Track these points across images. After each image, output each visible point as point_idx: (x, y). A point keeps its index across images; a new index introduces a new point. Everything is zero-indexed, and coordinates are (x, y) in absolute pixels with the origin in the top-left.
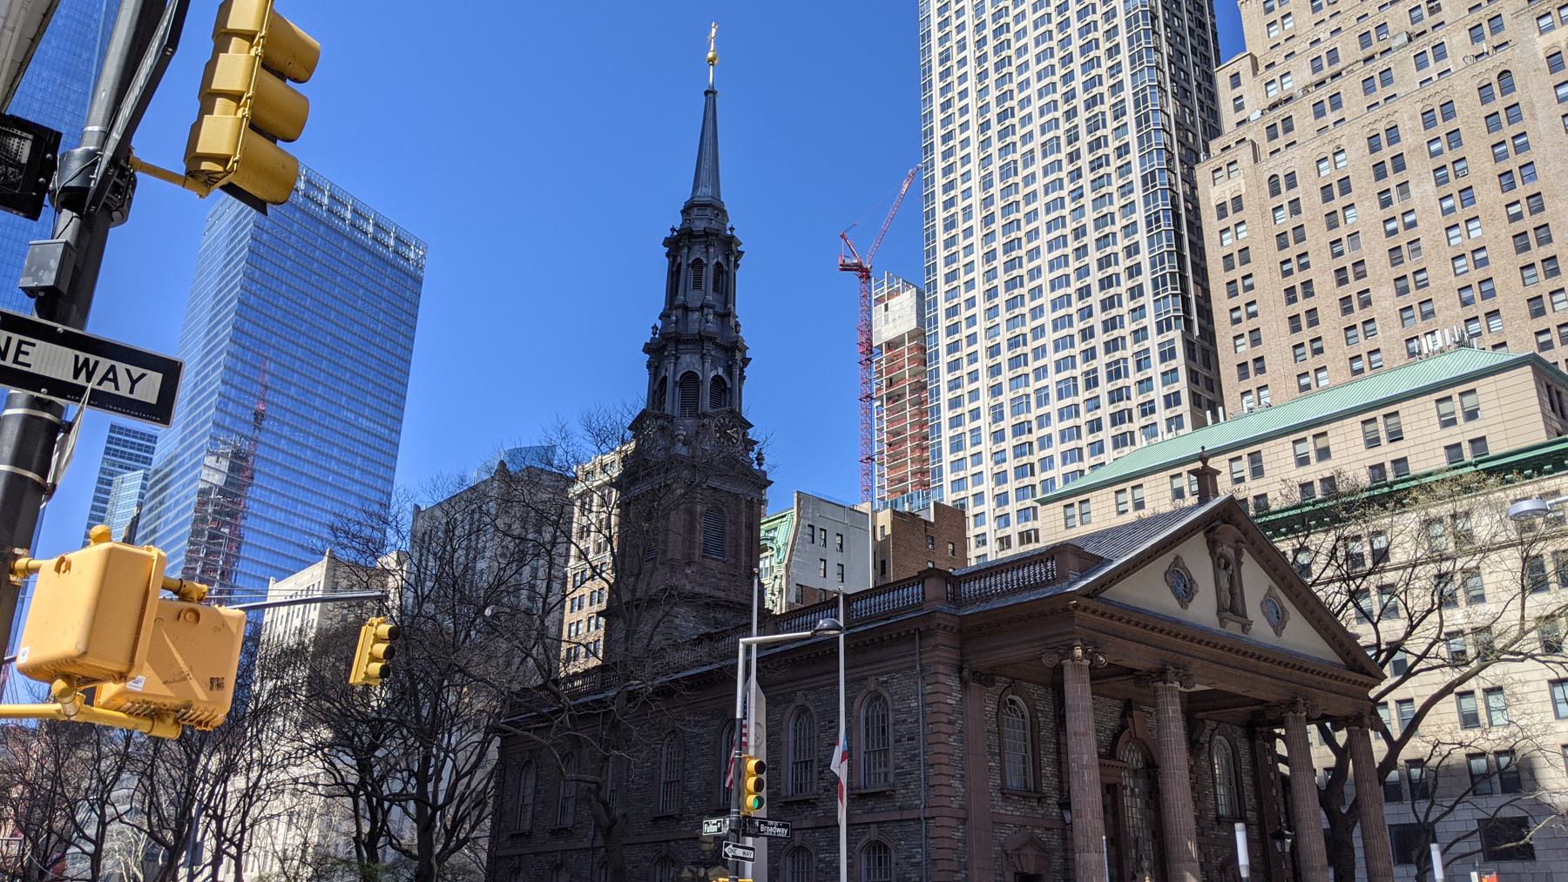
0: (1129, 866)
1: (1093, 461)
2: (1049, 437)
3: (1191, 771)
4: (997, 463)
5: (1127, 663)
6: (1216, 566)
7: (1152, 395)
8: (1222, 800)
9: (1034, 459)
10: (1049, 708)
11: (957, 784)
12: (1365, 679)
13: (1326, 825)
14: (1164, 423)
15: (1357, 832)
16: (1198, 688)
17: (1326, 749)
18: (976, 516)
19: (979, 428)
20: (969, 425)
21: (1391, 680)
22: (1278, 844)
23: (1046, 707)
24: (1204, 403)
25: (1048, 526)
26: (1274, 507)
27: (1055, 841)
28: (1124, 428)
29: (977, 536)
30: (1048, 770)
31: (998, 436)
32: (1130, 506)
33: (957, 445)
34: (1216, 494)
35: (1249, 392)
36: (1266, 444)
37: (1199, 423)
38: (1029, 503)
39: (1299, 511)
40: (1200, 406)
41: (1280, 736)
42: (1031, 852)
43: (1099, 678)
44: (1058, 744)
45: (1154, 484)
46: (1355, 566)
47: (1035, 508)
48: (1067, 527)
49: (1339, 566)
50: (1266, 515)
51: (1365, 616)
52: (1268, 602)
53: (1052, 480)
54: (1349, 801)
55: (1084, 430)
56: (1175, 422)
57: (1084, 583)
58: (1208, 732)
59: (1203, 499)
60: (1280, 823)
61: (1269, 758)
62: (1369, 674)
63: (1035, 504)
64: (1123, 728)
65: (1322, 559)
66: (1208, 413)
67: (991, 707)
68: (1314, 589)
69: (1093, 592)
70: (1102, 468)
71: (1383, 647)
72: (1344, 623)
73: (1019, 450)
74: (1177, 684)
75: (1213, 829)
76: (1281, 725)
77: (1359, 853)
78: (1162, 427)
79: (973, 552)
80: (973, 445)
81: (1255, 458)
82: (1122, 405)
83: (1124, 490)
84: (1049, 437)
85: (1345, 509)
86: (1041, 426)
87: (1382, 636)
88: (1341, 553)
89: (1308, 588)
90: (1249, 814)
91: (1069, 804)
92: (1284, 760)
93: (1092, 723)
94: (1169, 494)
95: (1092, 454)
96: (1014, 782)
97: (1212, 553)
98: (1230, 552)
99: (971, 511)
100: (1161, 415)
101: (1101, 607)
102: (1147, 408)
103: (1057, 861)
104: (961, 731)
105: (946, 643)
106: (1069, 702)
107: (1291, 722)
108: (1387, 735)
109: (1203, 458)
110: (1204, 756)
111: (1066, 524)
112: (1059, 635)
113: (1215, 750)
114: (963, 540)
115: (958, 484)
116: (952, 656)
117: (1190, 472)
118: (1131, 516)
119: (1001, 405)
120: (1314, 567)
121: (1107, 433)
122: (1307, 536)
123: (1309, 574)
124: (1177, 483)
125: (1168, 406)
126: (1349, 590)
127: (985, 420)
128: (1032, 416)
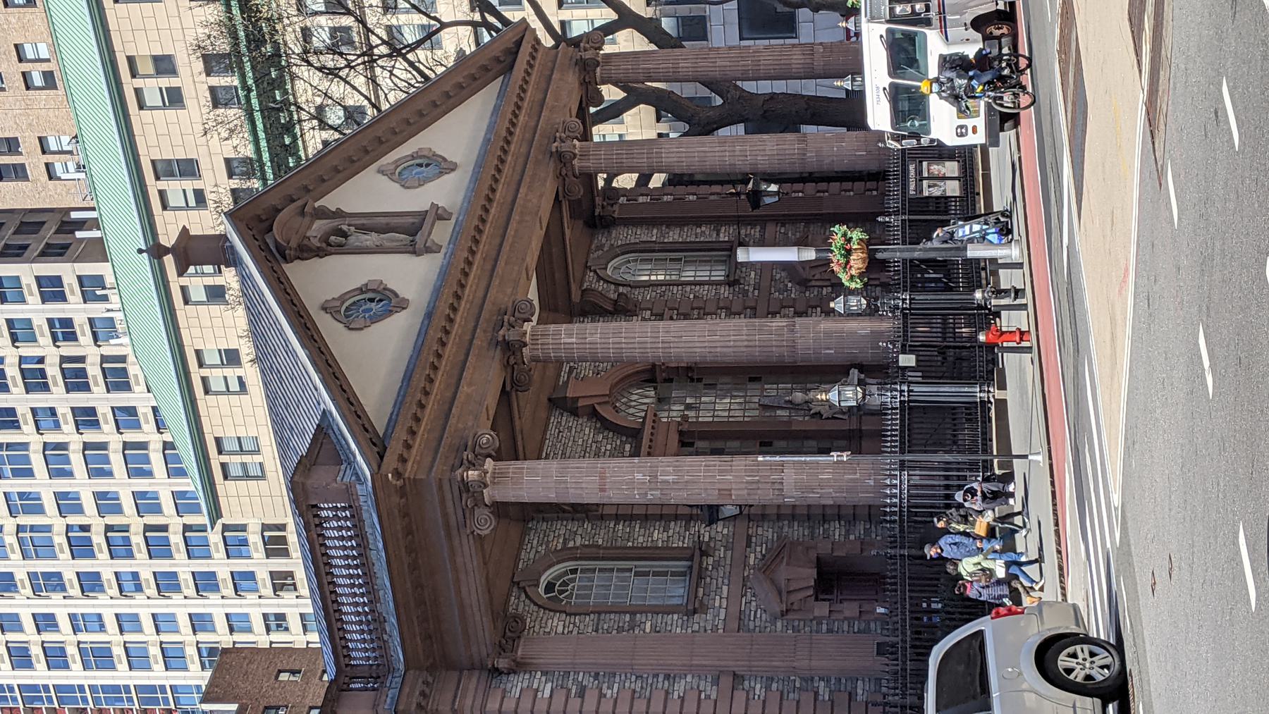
0: (801, 421)
1: (149, 426)
2: (99, 496)
3: (660, 317)
4: (139, 588)
5: (492, 400)
6: (341, 249)
7: (39, 322)
8: (703, 274)
9: (136, 524)
10: (561, 528)
11: (679, 688)
12: (526, 49)
13: (741, 128)
14: (89, 306)
15: (750, 86)
16: (533, 294)
17: (627, 116)
18: (232, 630)
19: (72, 617)
20: (65, 635)
21: (528, 13)
22: (768, 200)
23: (559, 533)
24: (61, 239)
25: (257, 508)
26: (249, 151)
27: (767, 533)
28: (93, 371)
29: (268, 630)
30: (658, 536)
31: (90, 583)
32: (232, 373)
33: (99, 657)
34: (224, 237)
35: (48, 166)
36: (142, 150)
37: (98, 251)
38: (215, 537)
39: (257, 115)
40: (66, 247)
41: (608, 181)
42: (783, 573)
43: (516, 451)
44: (617, 518)
45: (196, 332)
46: (351, 43)
47: (226, 528)
48: (262, 477)
49: (348, 66)
50: (262, 165)
51: (429, 37)
52: (400, 175)
53: (176, 495)
54: (704, 92)
55: (91, 436)
56: (91, 288)
57: (359, 458)
58: (601, 286)
59: (229, 258)
60: (738, 194)
61: (641, 199)
62: (519, 43)
63: (218, 527)
64: (594, 414)
65: (337, 89)
66: (79, 234)
67: (557, 623)
68: (385, 106)
69: (377, 446)
70: (164, 412)
71: (477, 17)
72: (440, 70)
73: (119, 547)
74: (527, 327)
75: (746, 293)
76: (590, 178)
77: (780, 87)
78: (97, 310)
79: (297, 637)
80: (102, 628)
81: (165, 169)
82: (53, 371)
83: (204, 380)
84: (99, 496)
85: (258, 47)
86: (79, 510)
87: (460, 17)
88: (329, 61)
89: (382, 117)
90: (723, 237)
91: (710, 507)
92: (644, 179)
93: (585, 463)
94: (215, 309)
95: (137, 426)
96: (677, 592)
97: (320, 253)
98: (319, 227)
99: (223, 638)
100: (76, 309)
101: (401, 434)
102: (63, 330)
103: (796, 532)
104: (597, 676)
105: (449, 696)
106: (551, 497)
107: (590, 164)
108: (609, 29)
109: (156, 251)
110: (637, 294)
111: (256, 478)
112: (443, 501)
113: (629, 278)
114: (273, 652)
115: (172, 658)
116: (472, 685)
117: (181, 273)
118: (251, 373)
119: (32, 576)
120: (350, 102)
121: (100, 398)
122: (299, 108)
123: (360, 110)
124: (198, 294)
125: (61, 297)
126: (390, 56)
127: (55, 605)
128: (59, 524)
